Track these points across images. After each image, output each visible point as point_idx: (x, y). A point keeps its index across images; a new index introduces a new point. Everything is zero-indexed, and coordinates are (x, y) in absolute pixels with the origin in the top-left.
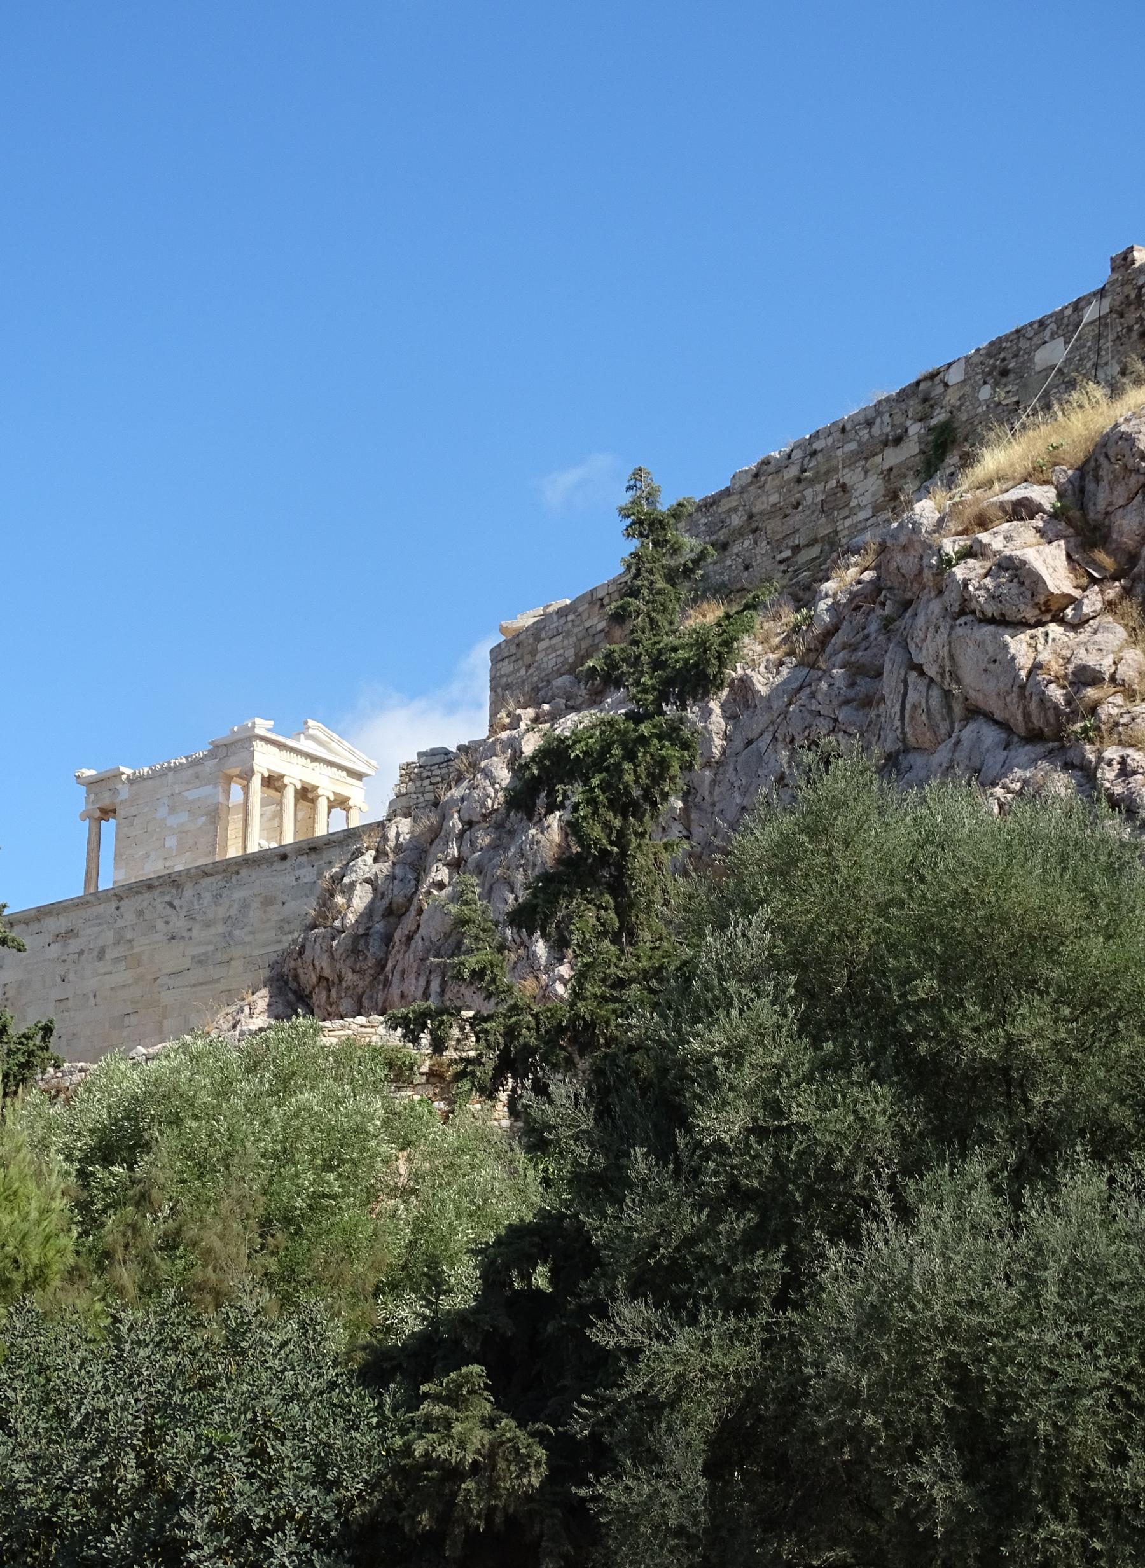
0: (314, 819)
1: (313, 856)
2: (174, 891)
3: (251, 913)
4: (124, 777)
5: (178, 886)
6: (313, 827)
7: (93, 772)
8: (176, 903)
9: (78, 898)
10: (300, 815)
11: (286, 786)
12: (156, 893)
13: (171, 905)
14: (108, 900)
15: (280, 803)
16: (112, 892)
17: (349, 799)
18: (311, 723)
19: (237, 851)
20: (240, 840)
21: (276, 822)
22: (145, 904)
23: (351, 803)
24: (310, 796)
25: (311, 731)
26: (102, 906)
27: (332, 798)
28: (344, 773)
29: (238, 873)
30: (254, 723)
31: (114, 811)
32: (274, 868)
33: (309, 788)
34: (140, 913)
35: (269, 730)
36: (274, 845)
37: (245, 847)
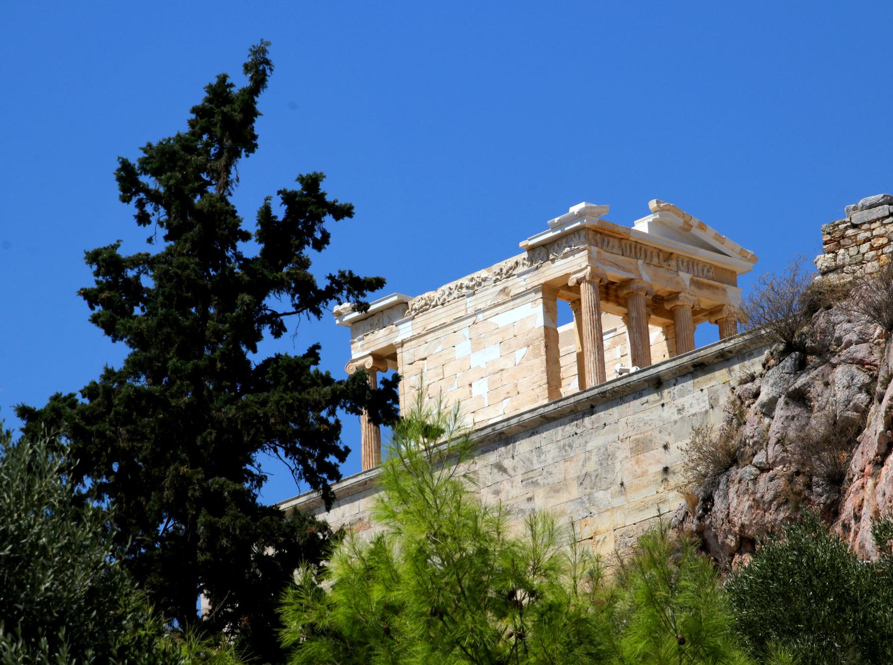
3: (618, 466)
13: (501, 468)
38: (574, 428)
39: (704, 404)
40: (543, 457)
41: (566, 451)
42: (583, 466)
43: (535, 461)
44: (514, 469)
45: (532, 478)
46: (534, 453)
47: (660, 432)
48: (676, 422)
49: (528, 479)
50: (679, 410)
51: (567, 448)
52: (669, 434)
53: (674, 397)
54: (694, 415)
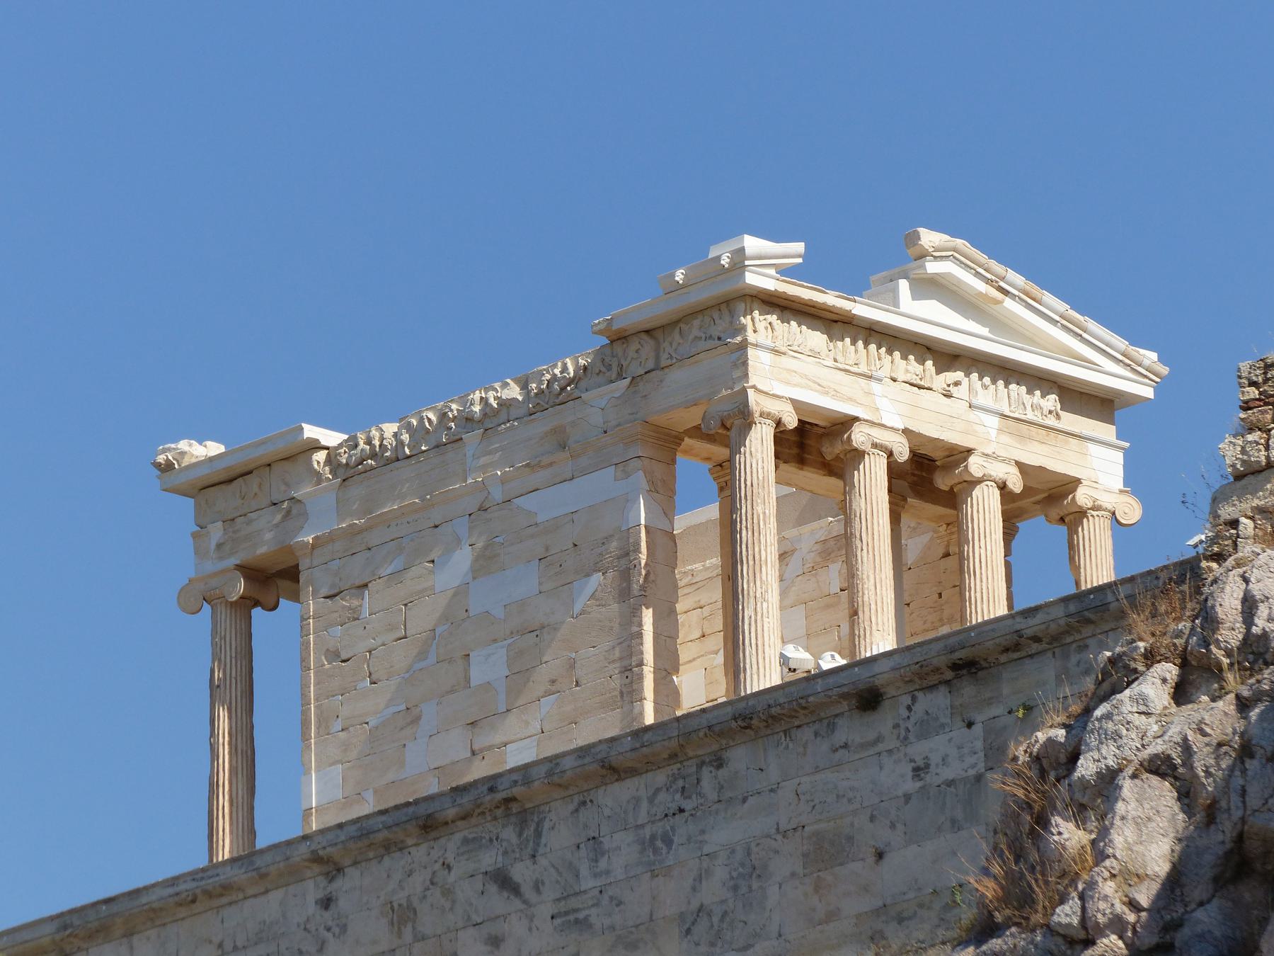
0: (962, 558)
1: (968, 691)
2: (509, 834)
3: (773, 893)
4: (320, 456)
5: (523, 818)
6: (960, 588)
7: (214, 448)
8: (521, 872)
9: (194, 875)
10: (914, 547)
11: (858, 455)
12: (450, 845)
13: (504, 881)
14: (292, 875)
15: (844, 509)
16: (304, 849)
17: (1076, 482)
18: (929, 238)
19: (710, 683)
20: (717, 641)
21: (833, 577)
22: (418, 881)
23: (1082, 497)
24: (943, 482)
25: (932, 267)
26: (275, 896)
27: (1016, 484)
28: (1052, 401)
29: (719, 763)
30: (740, 253)
31: (292, 574)
32: (840, 736)
33: (936, 455)
34: (402, 916)
35: (787, 272)
36: (831, 661)
37: (734, 667)
38: (678, 796)
39: (972, 760)
40: (603, 864)
41: (656, 851)
42: (694, 889)
43: (584, 871)
44: (537, 886)
45: (576, 910)
46: (583, 852)
47: (872, 818)
48: (907, 797)
49: (567, 913)
50: (917, 770)
51: (659, 843)
52: (893, 826)
53: (906, 738)
54: (950, 783)
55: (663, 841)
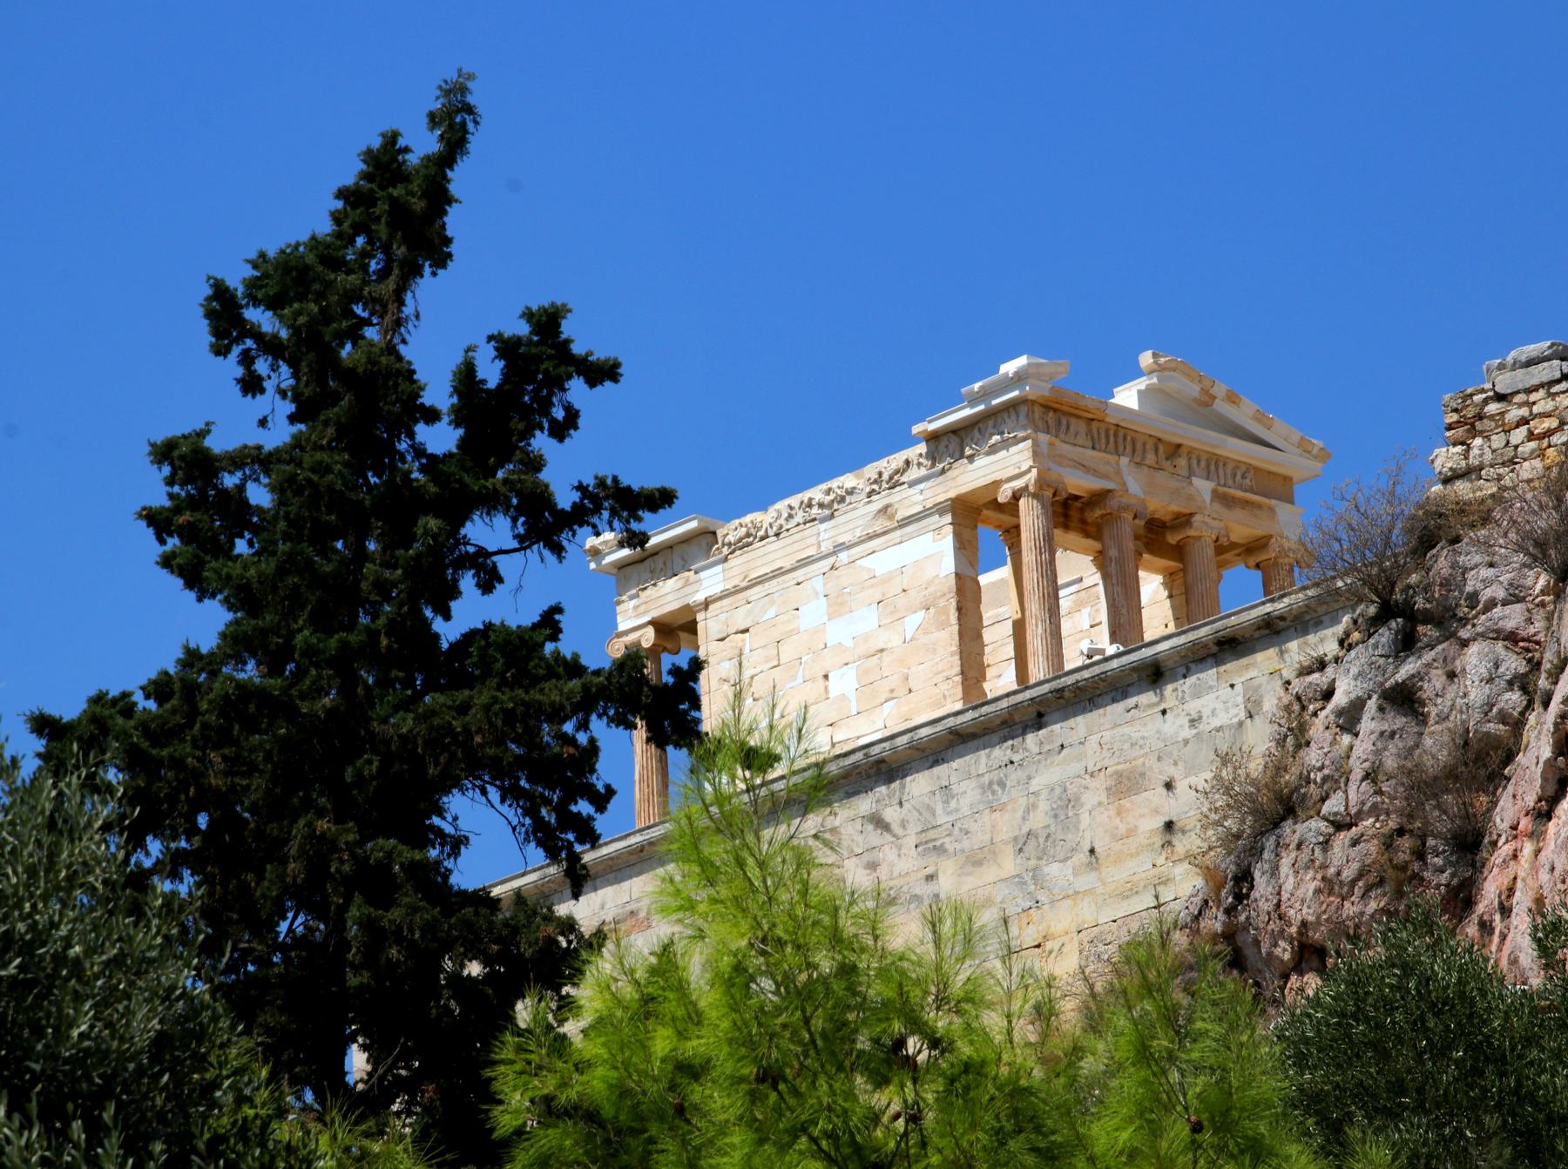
3: (1085, 819)
13: (879, 823)
38: (1009, 752)
39: (1236, 711)
40: (953, 804)
41: (993, 793)
42: (1024, 818)
43: (939, 811)
44: (903, 824)
45: (934, 840)
46: (938, 796)
47: (1159, 759)
48: (1186, 742)
49: (926, 842)
50: (1192, 721)
51: (995, 787)
52: (1175, 764)
53: (1183, 698)
54: (1218, 729)
55: (999, 784)
